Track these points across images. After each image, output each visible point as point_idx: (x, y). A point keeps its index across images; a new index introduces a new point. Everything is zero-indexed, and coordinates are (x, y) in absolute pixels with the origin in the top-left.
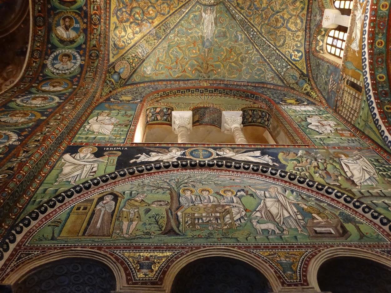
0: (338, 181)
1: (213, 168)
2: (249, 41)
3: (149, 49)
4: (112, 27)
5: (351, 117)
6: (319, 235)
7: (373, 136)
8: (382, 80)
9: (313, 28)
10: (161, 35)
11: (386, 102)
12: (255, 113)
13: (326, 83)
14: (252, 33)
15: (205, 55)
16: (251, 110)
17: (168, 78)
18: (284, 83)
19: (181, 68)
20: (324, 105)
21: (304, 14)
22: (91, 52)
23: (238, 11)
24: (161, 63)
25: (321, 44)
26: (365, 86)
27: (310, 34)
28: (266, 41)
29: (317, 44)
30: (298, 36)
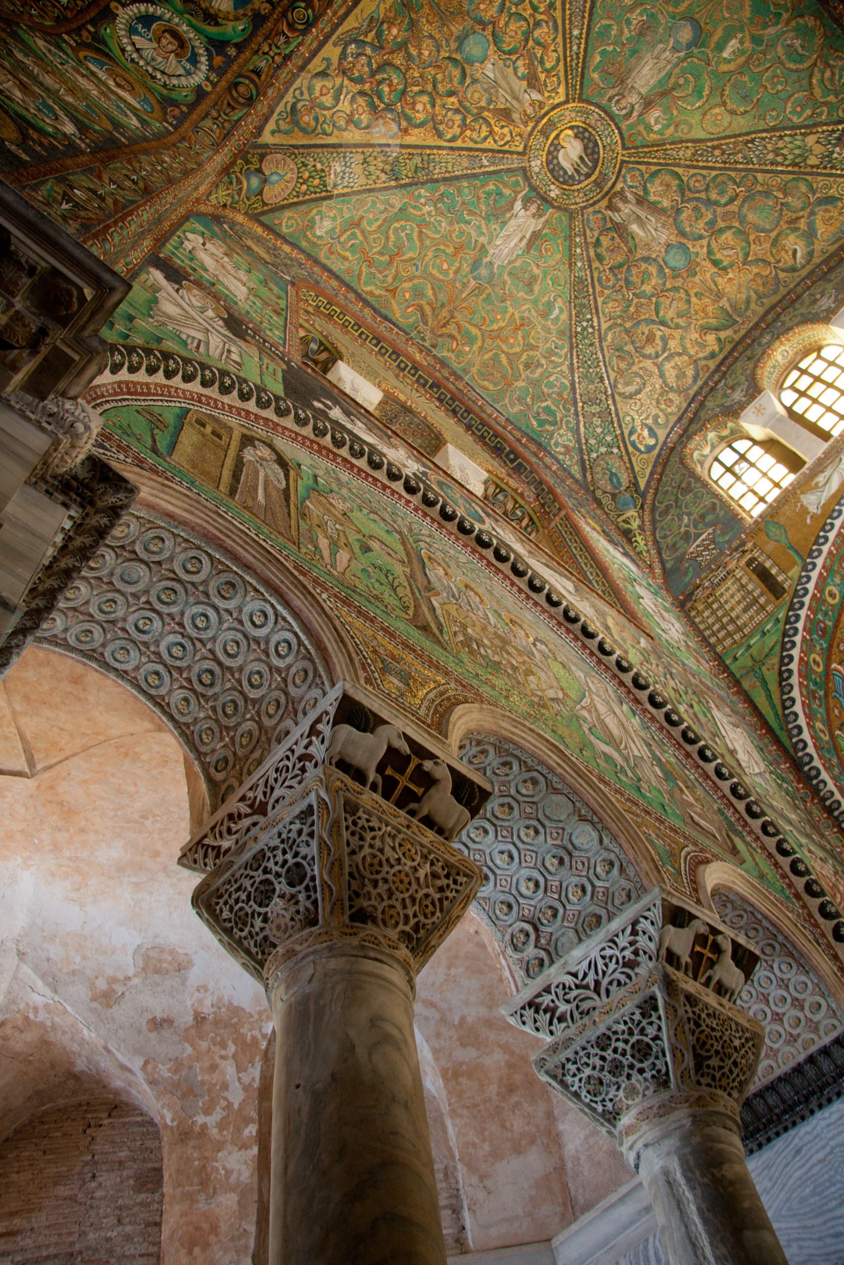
1: (484, 552)
2: (572, 337)
3: (359, 181)
4: (316, 65)
5: (720, 635)
7: (760, 699)
8: (830, 600)
9: (713, 409)
10: (404, 172)
11: (818, 648)
12: (500, 497)
13: (686, 537)
14: (585, 324)
15: (462, 291)
16: (497, 486)
17: (347, 279)
18: (585, 476)
19: (390, 279)
20: (654, 578)
21: (708, 368)
22: (240, 80)
23: (588, 256)
25: (707, 451)
26: (796, 590)
27: (695, 414)
28: (601, 364)
30: (671, 401)
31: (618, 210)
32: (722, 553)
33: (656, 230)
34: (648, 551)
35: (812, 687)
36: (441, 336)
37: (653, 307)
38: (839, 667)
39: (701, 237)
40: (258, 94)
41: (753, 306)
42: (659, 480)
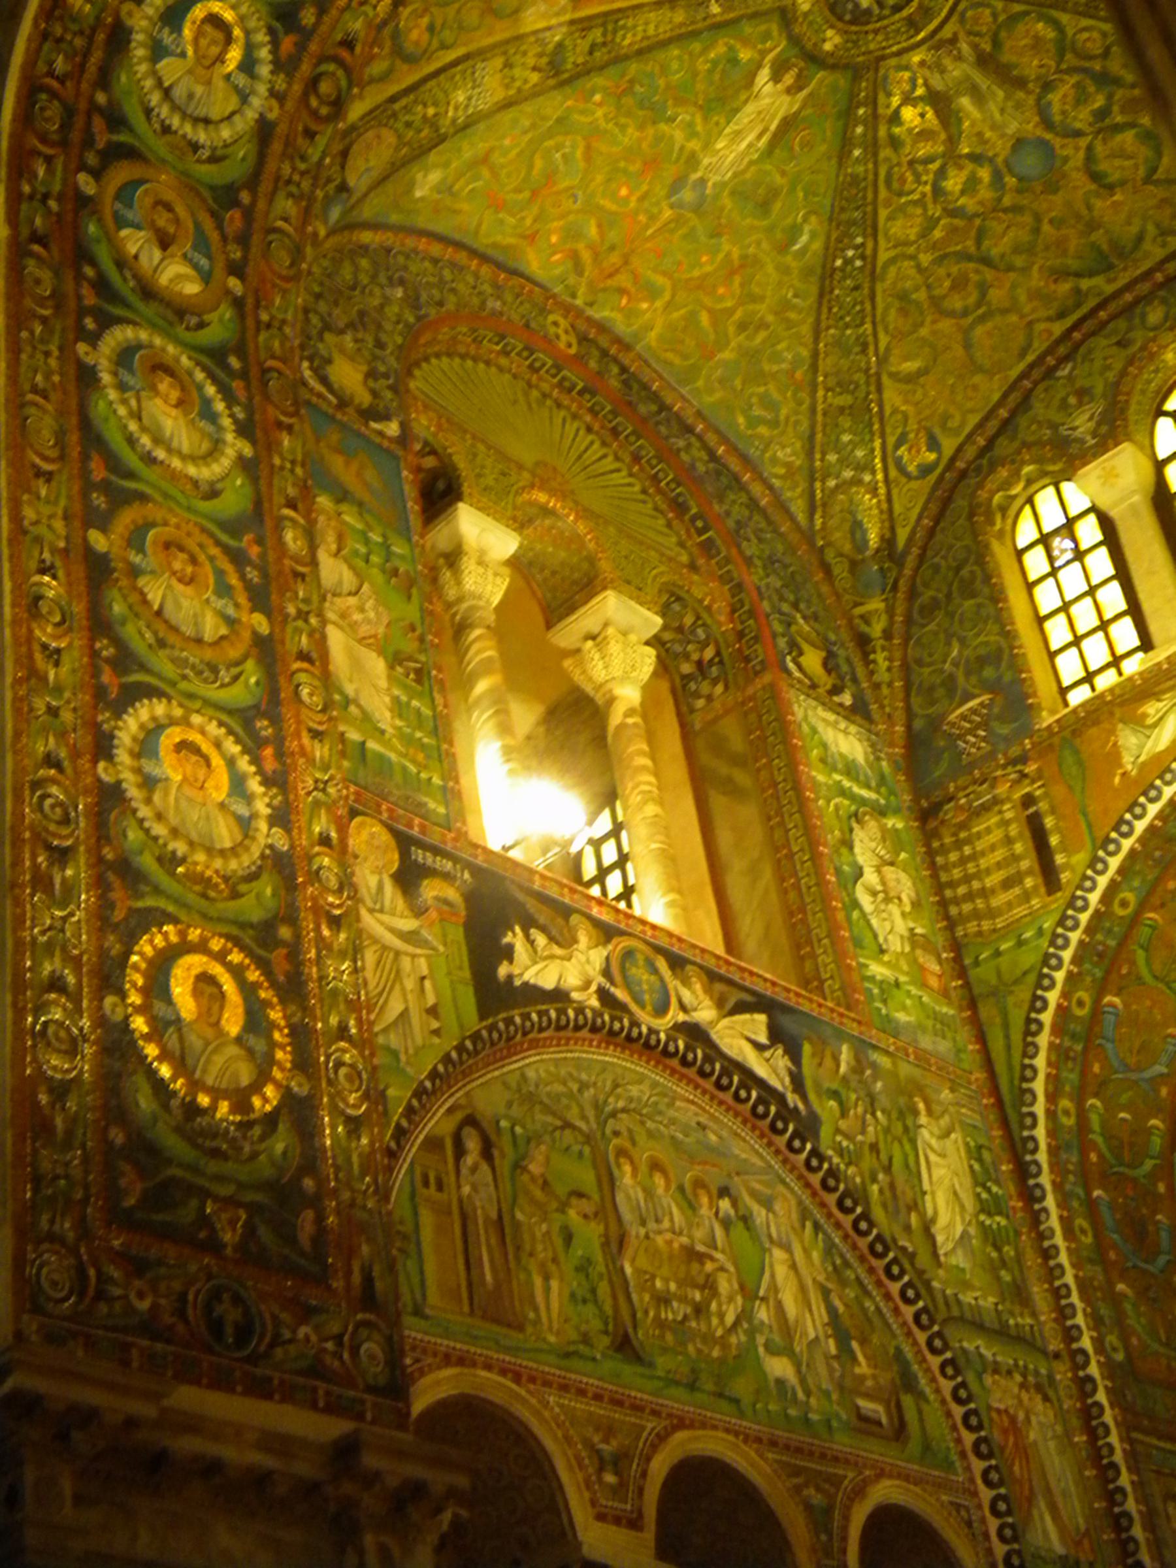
0: (907, 1228)
1: (668, 1061)
6: (863, 1425)
8: (1121, 912)
14: (850, 253)
15: (647, 227)
17: (457, 237)
19: (528, 222)
20: (892, 745)
21: (1050, 333)
24: (485, 172)
25: (1017, 489)
26: (1074, 898)
27: (1014, 413)
29: (1007, 485)
30: (975, 388)
31: (942, 71)
32: (992, 755)
33: (1002, 111)
34: (890, 684)
35: (1067, 1043)
36: (605, 290)
37: (973, 233)
38: (1116, 1000)
39: (1078, 134)
40: (350, 86)
41: (1147, 245)
42: (931, 532)
